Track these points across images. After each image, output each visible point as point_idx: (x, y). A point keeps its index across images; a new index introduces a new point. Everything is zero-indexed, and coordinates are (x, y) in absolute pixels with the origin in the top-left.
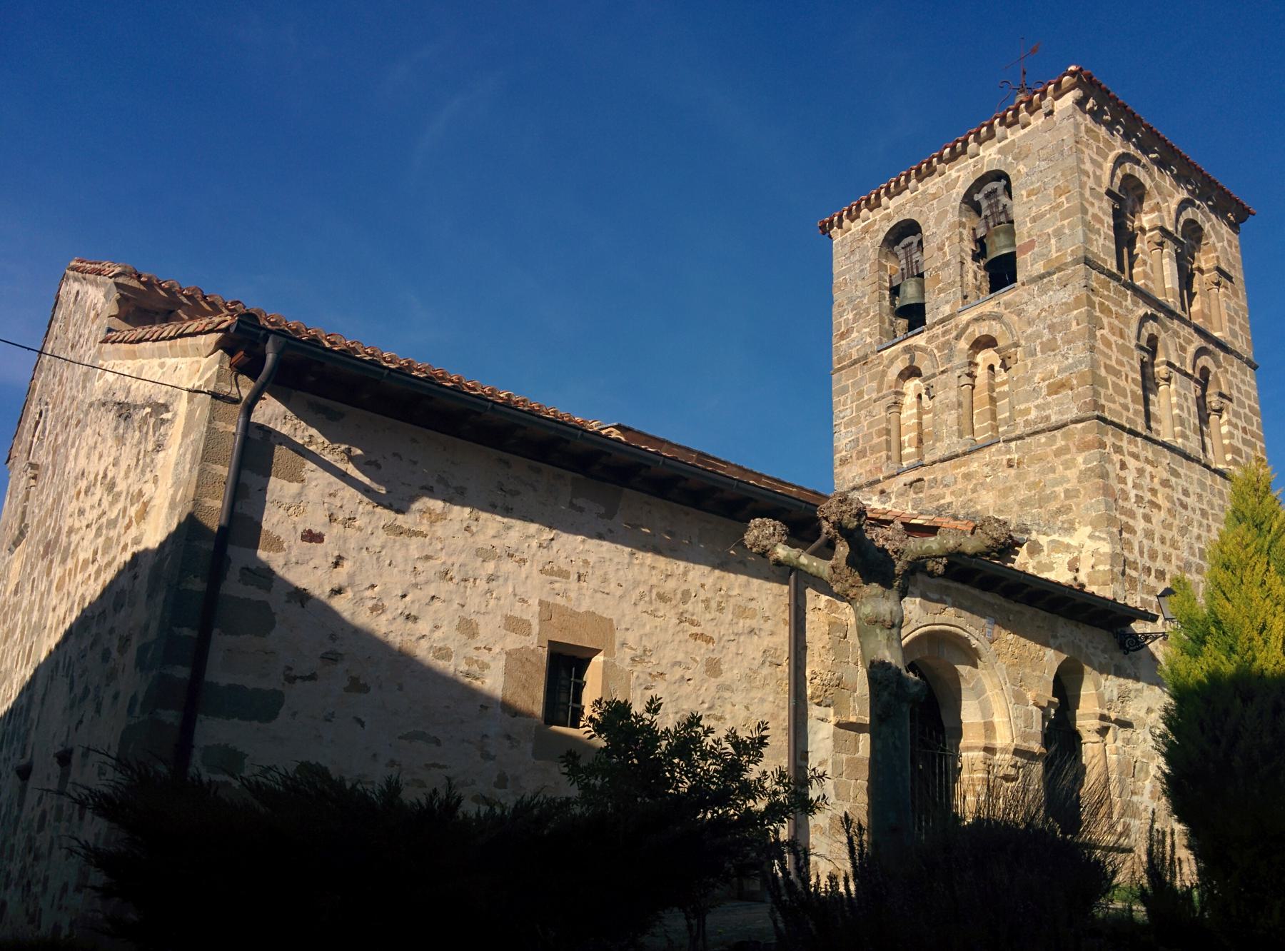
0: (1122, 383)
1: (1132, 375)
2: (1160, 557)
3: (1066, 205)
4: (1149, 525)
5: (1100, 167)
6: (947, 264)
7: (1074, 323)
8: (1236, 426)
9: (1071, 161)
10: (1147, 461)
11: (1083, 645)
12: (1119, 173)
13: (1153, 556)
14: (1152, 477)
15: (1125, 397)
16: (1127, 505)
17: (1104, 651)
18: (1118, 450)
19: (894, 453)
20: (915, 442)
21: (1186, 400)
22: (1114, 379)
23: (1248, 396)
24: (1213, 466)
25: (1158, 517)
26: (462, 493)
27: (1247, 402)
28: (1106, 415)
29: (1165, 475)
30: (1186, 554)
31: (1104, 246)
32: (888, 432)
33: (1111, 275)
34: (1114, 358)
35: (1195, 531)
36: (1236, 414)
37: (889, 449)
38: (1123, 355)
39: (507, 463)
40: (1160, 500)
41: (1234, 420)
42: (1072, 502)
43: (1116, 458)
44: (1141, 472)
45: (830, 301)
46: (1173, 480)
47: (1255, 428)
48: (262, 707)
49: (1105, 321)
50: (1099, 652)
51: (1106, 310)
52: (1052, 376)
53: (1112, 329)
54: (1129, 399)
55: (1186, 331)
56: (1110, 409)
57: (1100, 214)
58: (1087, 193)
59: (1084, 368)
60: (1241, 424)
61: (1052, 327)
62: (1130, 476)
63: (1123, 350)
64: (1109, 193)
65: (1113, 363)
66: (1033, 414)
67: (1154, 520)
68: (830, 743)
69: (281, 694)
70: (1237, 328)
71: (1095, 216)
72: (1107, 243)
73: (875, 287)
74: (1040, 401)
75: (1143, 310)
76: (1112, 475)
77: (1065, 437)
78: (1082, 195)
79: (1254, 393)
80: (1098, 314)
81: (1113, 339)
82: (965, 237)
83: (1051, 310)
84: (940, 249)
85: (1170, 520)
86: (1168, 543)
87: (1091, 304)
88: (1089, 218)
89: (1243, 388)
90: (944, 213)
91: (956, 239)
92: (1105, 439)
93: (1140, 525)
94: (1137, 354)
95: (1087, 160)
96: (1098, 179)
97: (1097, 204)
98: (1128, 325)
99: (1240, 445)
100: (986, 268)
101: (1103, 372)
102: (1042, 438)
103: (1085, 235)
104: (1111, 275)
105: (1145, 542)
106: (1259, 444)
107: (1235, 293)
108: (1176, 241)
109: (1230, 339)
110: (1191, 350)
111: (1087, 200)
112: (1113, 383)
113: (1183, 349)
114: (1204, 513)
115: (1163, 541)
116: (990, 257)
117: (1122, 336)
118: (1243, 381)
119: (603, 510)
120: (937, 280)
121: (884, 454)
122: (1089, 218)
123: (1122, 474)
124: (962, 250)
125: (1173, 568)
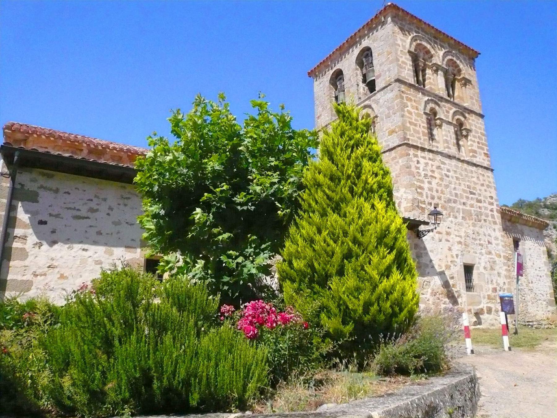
0: (417, 128)
1: (422, 125)
2: (436, 198)
4: (430, 186)
5: (405, 42)
6: (352, 86)
8: (474, 141)
12: (414, 44)
13: (433, 198)
14: (432, 165)
16: (421, 178)
18: (416, 156)
21: (449, 132)
22: (414, 127)
23: (480, 128)
24: (462, 159)
25: (434, 182)
26: (105, 200)
27: (479, 131)
28: (410, 142)
30: (448, 196)
31: (408, 75)
33: (411, 86)
34: (413, 119)
35: (453, 186)
36: (474, 137)
38: (418, 117)
39: (124, 187)
40: (436, 175)
42: (398, 179)
43: (415, 159)
44: (427, 164)
46: (442, 166)
47: (483, 142)
48: (26, 286)
49: (409, 104)
51: (410, 100)
52: (390, 128)
53: (412, 107)
54: (421, 135)
55: (448, 105)
56: (412, 140)
57: (406, 61)
58: (399, 53)
59: (400, 124)
60: (477, 140)
61: (389, 108)
62: (421, 166)
63: (418, 115)
64: (409, 52)
65: (413, 121)
66: (384, 144)
67: (433, 183)
69: (32, 282)
70: (474, 101)
71: (403, 62)
72: (409, 72)
73: (328, 97)
74: (386, 139)
75: (426, 98)
76: (413, 167)
77: (395, 153)
78: (396, 54)
79: (483, 127)
80: (405, 101)
81: (413, 111)
82: (358, 74)
83: (387, 101)
84: (350, 80)
85: (441, 182)
86: (440, 192)
87: (402, 98)
88: (400, 63)
89: (478, 125)
90: (350, 65)
91: (355, 75)
92: (410, 152)
93: (426, 186)
94: (424, 116)
96: (404, 47)
97: (404, 57)
98: (420, 104)
99: (476, 149)
100: (367, 85)
101: (408, 125)
102: (387, 154)
103: (398, 70)
104: (411, 86)
105: (429, 192)
106: (485, 148)
107: (474, 88)
108: (443, 69)
109: (471, 106)
110: (452, 112)
111: (399, 56)
112: (413, 129)
113: (448, 112)
114: (457, 178)
115: (437, 191)
116: (368, 81)
117: (417, 109)
118: (477, 123)
120: (349, 92)
122: (400, 63)
123: (418, 165)
124: (357, 79)
125: (442, 202)
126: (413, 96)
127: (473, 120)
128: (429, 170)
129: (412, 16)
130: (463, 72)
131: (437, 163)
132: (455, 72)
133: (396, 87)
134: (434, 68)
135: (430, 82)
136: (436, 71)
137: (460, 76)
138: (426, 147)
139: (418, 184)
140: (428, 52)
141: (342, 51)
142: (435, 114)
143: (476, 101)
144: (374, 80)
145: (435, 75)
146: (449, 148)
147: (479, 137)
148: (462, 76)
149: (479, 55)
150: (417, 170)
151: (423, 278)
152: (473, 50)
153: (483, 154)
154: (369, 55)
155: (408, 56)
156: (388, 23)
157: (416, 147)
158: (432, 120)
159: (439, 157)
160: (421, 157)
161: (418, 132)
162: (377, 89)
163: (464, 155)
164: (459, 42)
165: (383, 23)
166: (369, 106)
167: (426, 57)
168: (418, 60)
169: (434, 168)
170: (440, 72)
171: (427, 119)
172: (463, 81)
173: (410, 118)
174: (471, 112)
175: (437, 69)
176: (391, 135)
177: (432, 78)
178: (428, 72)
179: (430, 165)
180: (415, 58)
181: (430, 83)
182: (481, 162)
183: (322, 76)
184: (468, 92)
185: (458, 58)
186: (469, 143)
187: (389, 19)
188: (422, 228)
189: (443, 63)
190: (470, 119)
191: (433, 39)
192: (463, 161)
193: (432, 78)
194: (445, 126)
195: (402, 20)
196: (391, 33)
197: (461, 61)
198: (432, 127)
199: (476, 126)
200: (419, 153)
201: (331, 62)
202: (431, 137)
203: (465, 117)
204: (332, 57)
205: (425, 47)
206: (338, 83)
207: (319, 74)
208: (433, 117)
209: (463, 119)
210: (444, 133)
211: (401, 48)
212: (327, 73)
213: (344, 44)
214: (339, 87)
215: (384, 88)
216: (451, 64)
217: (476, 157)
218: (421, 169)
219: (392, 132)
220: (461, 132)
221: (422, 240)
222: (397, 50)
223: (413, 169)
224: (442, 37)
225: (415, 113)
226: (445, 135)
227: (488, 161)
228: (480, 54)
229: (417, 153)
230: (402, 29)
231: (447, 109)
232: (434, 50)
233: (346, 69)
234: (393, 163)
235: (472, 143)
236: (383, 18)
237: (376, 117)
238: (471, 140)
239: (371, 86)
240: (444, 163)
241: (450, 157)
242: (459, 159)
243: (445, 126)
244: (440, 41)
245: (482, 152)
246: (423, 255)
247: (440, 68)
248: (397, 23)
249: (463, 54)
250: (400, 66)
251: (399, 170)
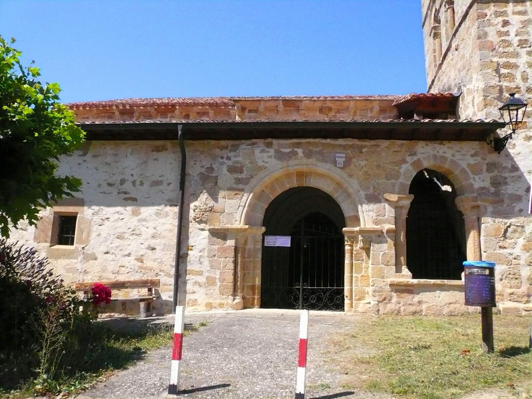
11: (448, 155)
16: (511, 49)
17: (472, 156)
50: (468, 157)
68: (206, 240)
92: (486, 11)
119: (81, 153)
123: (505, 29)
139: (502, 61)
151: (505, 221)
188: (502, 133)
218: (513, 34)
221: (508, 155)
246: (509, 180)
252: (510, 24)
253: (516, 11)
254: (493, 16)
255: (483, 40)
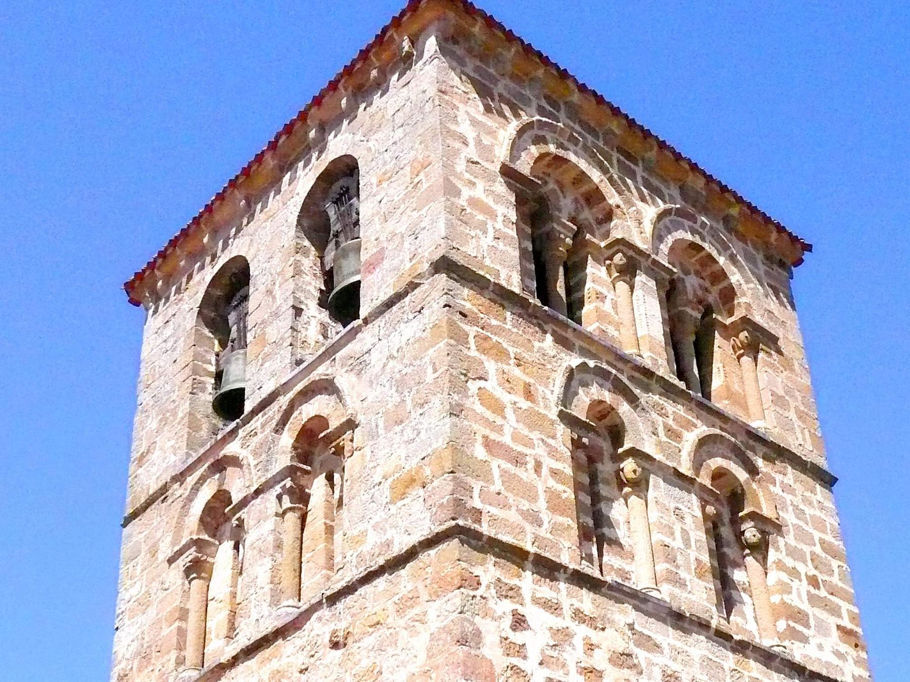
0: (526, 474)
1: (549, 463)
3: (425, 186)
6: (276, 315)
7: (430, 370)
8: (794, 573)
9: (433, 120)
10: (579, 616)
12: (535, 151)
14: (591, 647)
15: (534, 499)
18: (510, 592)
19: (190, 653)
20: (224, 631)
23: (820, 525)
27: (817, 535)
28: (485, 529)
29: (621, 646)
31: (500, 254)
32: (183, 614)
33: (503, 297)
34: (508, 430)
36: (793, 552)
37: (181, 647)
38: (532, 427)
41: (790, 562)
43: (506, 606)
44: (562, 637)
45: (131, 405)
46: (641, 655)
47: (835, 580)
49: (491, 366)
51: (501, 354)
53: (507, 381)
56: (494, 520)
57: (490, 201)
58: (461, 166)
59: (440, 443)
61: (400, 385)
63: (534, 420)
64: (508, 173)
65: (507, 439)
66: (373, 539)
70: (792, 415)
72: (501, 245)
73: (188, 371)
75: (575, 361)
79: (832, 521)
80: (473, 353)
81: (506, 398)
84: (269, 292)
87: (461, 338)
88: (462, 202)
89: (809, 511)
91: (290, 272)
92: (478, 571)
94: (563, 432)
95: (462, 116)
96: (486, 151)
97: (481, 185)
98: (546, 380)
99: (805, 606)
101: (480, 452)
102: (381, 583)
103: (449, 225)
104: (503, 297)
106: (845, 606)
108: (655, 269)
110: (690, 438)
111: (459, 177)
112: (504, 473)
117: (528, 394)
118: (805, 500)
120: (262, 340)
121: (173, 655)
122: (462, 202)
123: (518, 637)
126: (515, 343)
127: (786, 488)
128: (572, 668)
129: (528, 49)
130: (741, 300)
131: (612, 640)
132: (712, 298)
133: (436, 294)
134: (619, 259)
135: (597, 309)
136: (628, 272)
137: (731, 314)
138: (567, 554)
140: (594, 197)
141: (251, 185)
142: (616, 434)
143: (801, 416)
144: (359, 282)
145: (622, 286)
146: (682, 584)
147: (814, 558)
148: (738, 314)
149: (807, 256)
150: (516, 661)
152: (780, 229)
153: (835, 633)
154: (352, 191)
155: (500, 187)
156: (426, 55)
157: (514, 555)
158: (599, 459)
159: (624, 614)
160: (536, 601)
161: (530, 493)
162: (364, 312)
163: (751, 626)
164: (724, 189)
165: (406, 62)
166: (327, 387)
167: (587, 215)
168: (551, 218)
169: (600, 660)
170: (641, 278)
171: (577, 444)
172: (743, 335)
173: (490, 424)
174: (779, 453)
175: (631, 264)
176: (403, 496)
177: (610, 296)
178: (596, 275)
179: (578, 642)
180: (534, 207)
181: (602, 316)
182: (828, 664)
183: (178, 291)
184: (763, 377)
185: (724, 248)
186: (774, 576)
187: (431, 44)
189: (657, 251)
190: (774, 483)
191: (615, 155)
192: (742, 648)
193: (610, 296)
194: (658, 487)
195: (483, 58)
196: (432, 91)
197: (732, 259)
198: (604, 490)
199: (799, 513)
200: (528, 582)
201: (215, 233)
202: (596, 530)
203: (753, 471)
204: (218, 217)
205: (582, 177)
206: (232, 317)
207: (167, 285)
208: (605, 445)
209: (742, 475)
210: (654, 514)
211: (471, 152)
212: (197, 278)
213: (259, 158)
214: (234, 334)
215: (389, 304)
216: (693, 261)
217: (805, 640)
218: (534, 655)
219: (406, 484)
220: (734, 532)
222: (450, 156)
223: (491, 650)
224: (652, 154)
225: (516, 409)
226: (658, 532)
227: (857, 662)
228: (808, 248)
229: (514, 582)
230: (484, 92)
231: (670, 422)
232: (620, 193)
233: (262, 256)
234: (402, 622)
235: (785, 577)
236: (406, 45)
237: (351, 425)
238: (780, 565)
239: (343, 304)
240: (645, 642)
241: (678, 619)
242: (722, 637)
243: (658, 487)
244: (646, 169)
245: (832, 621)
247: (644, 263)
248: (461, 62)
249: (742, 238)
250: (459, 215)
251: (422, 656)
252: (528, 628)
253: (538, 595)
254: (493, 591)
255: (473, 652)
